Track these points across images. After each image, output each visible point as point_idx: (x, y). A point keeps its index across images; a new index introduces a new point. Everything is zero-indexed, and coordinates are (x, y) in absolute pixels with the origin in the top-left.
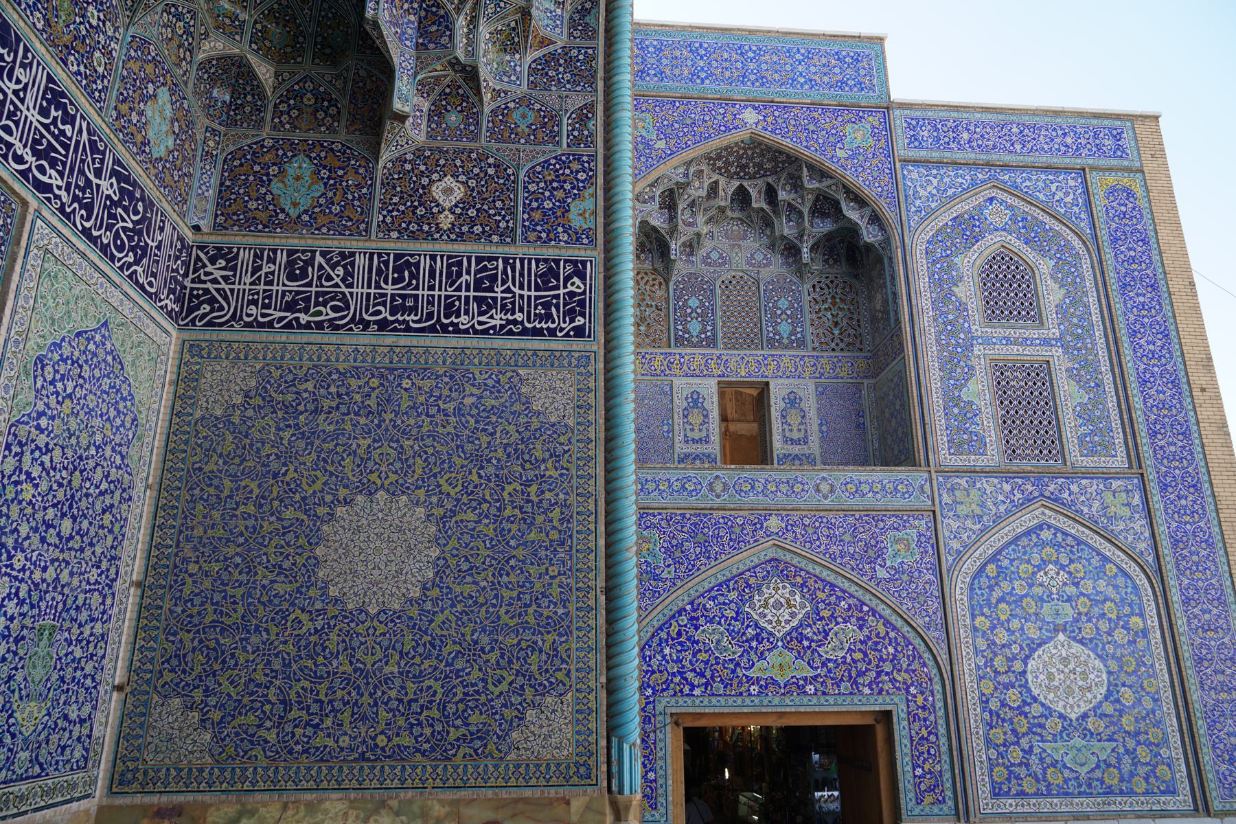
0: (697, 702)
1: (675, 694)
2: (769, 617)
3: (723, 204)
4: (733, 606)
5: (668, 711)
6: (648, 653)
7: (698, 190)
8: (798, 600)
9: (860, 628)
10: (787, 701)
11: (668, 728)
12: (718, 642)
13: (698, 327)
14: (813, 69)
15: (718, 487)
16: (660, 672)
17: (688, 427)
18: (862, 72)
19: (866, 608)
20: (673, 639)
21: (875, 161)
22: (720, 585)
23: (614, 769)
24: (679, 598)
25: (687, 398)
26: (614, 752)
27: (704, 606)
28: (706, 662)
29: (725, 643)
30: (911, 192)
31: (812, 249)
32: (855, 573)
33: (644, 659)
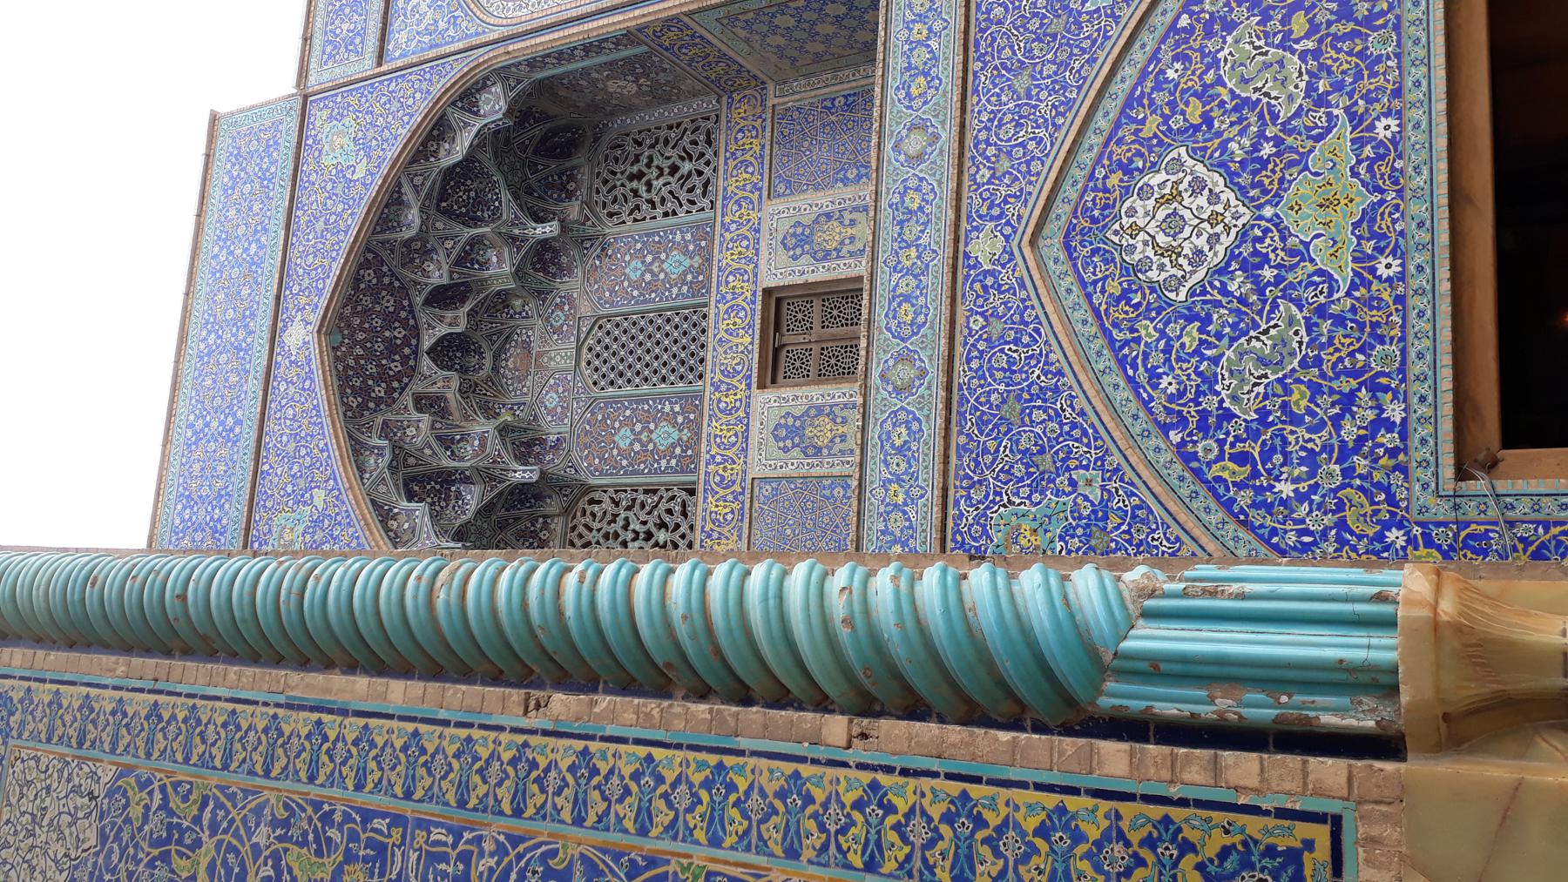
0: (1424, 410)
1: (1403, 469)
2: (1201, 242)
3: (455, 384)
4: (1173, 330)
5: (1448, 486)
6: (1292, 538)
7: (419, 429)
8: (1162, 177)
9: (1230, 26)
10: (1419, 181)
11: (1503, 486)
12: (1262, 361)
13: (665, 427)
14: (241, 230)
15: (905, 373)
16: (1340, 506)
17: (838, 446)
18: (254, 145)
19: (1184, 21)
20: (1255, 474)
21: (378, 109)
22: (1122, 362)
23: (1259, 709)
24: (1151, 460)
25: (785, 450)
26: (1171, 704)
27: (1171, 398)
28: (1315, 389)
29: (1264, 346)
30: (426, 39)
31: (539, 220)
32: (1102, 55)
33: (1306, 548)
